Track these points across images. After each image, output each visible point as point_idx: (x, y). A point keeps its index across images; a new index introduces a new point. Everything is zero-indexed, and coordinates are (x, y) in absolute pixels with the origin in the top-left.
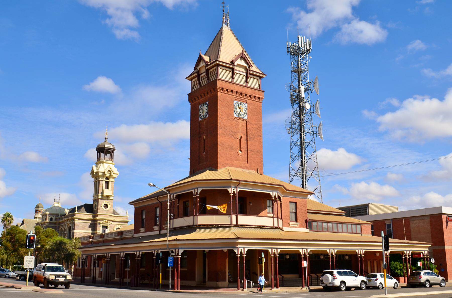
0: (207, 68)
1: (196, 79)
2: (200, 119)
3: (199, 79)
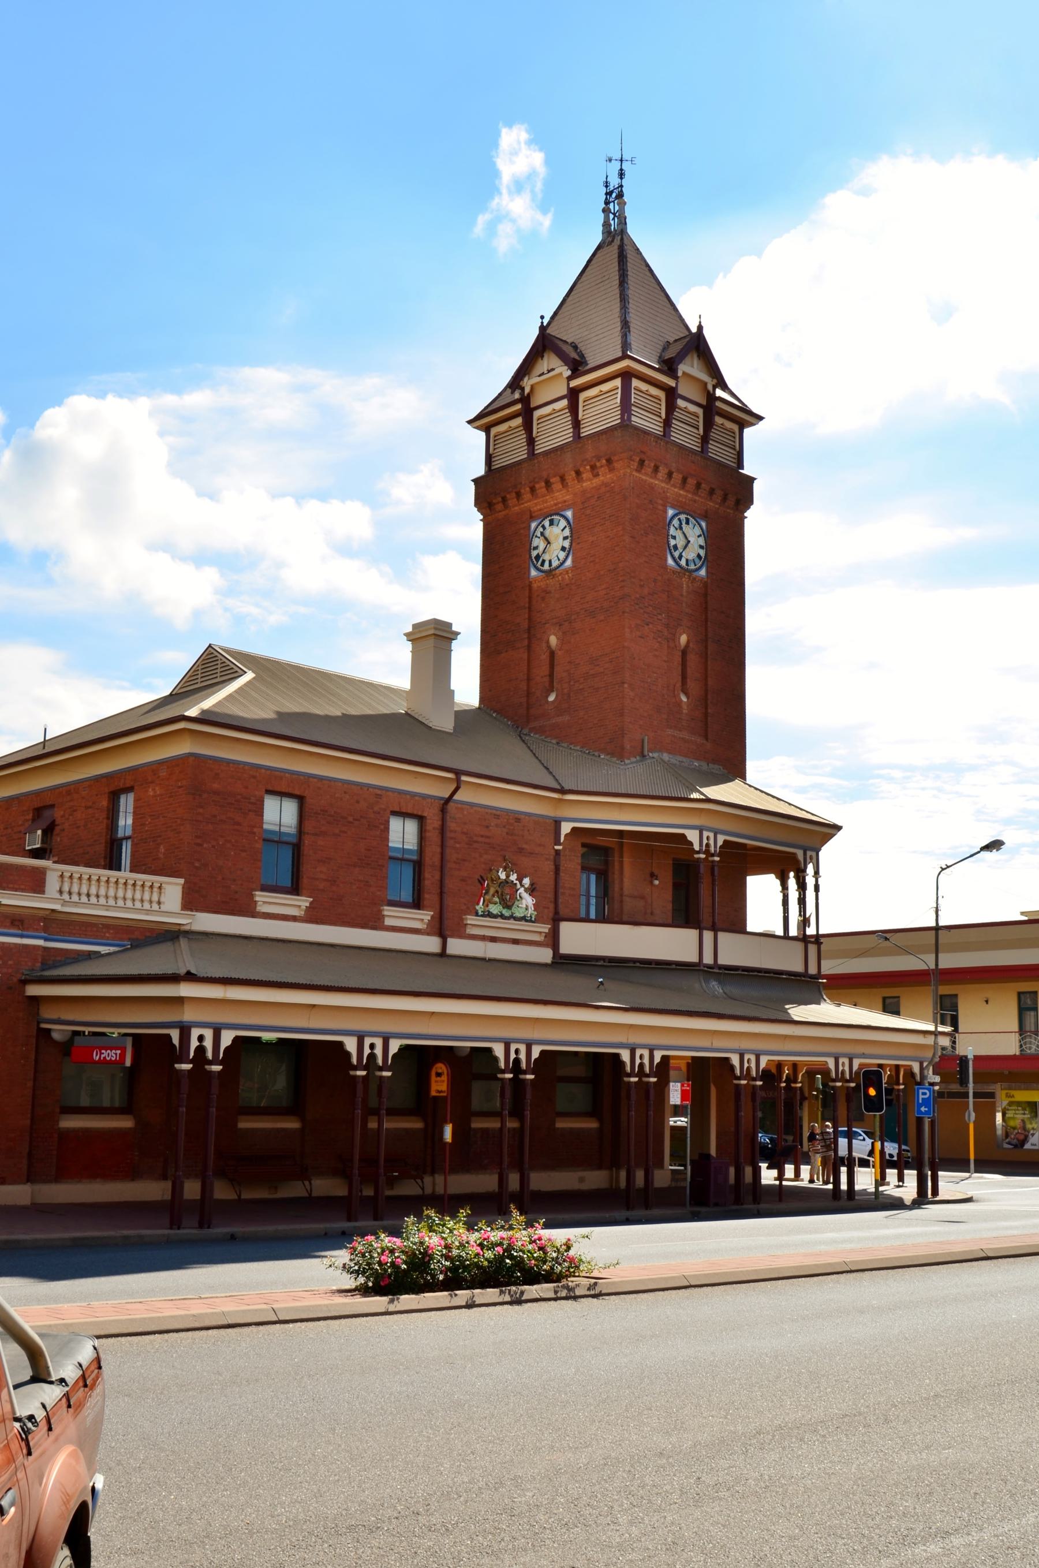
0: (574, 383)
1: (519, 421)
2: (534, 573)
3: (528, 426)
